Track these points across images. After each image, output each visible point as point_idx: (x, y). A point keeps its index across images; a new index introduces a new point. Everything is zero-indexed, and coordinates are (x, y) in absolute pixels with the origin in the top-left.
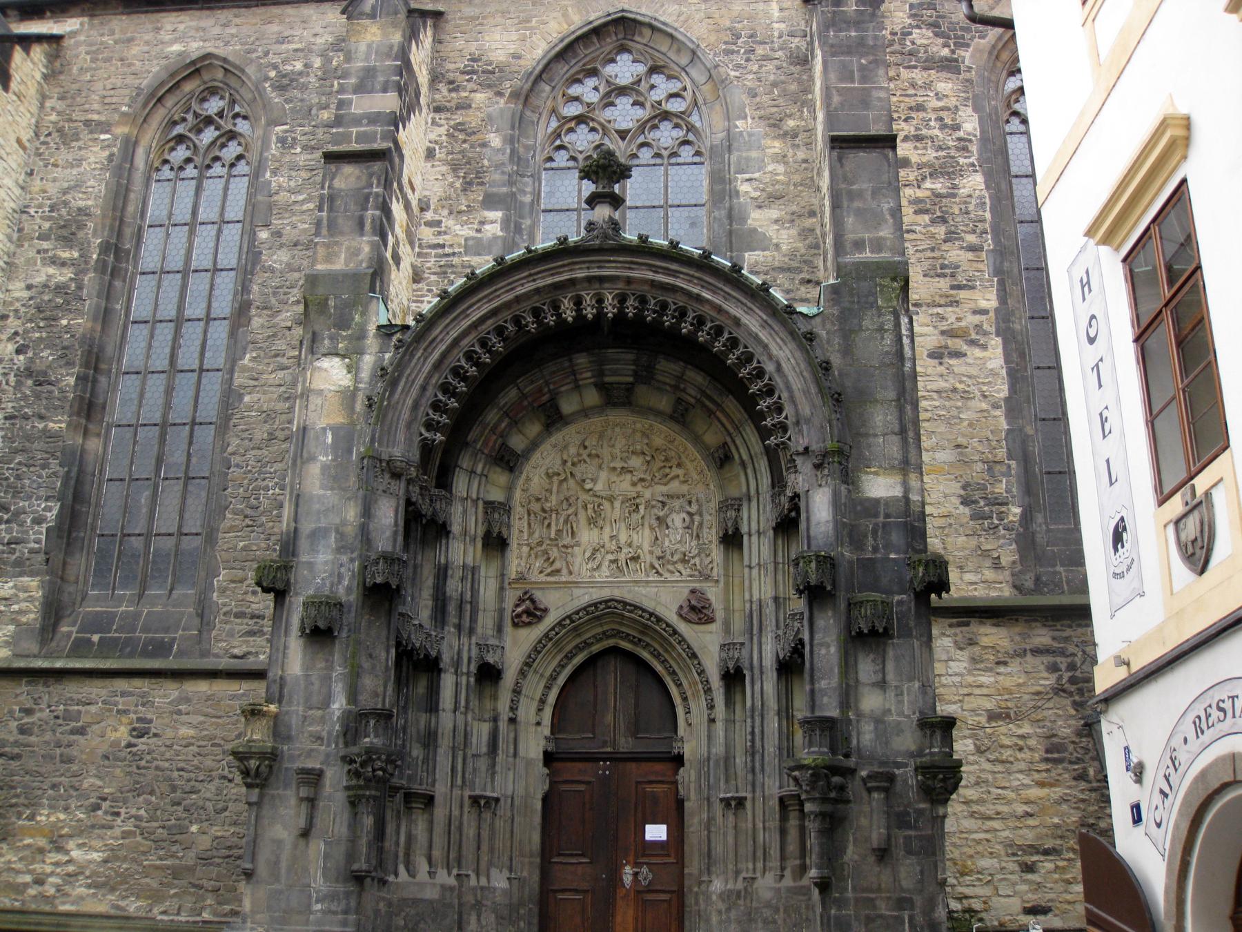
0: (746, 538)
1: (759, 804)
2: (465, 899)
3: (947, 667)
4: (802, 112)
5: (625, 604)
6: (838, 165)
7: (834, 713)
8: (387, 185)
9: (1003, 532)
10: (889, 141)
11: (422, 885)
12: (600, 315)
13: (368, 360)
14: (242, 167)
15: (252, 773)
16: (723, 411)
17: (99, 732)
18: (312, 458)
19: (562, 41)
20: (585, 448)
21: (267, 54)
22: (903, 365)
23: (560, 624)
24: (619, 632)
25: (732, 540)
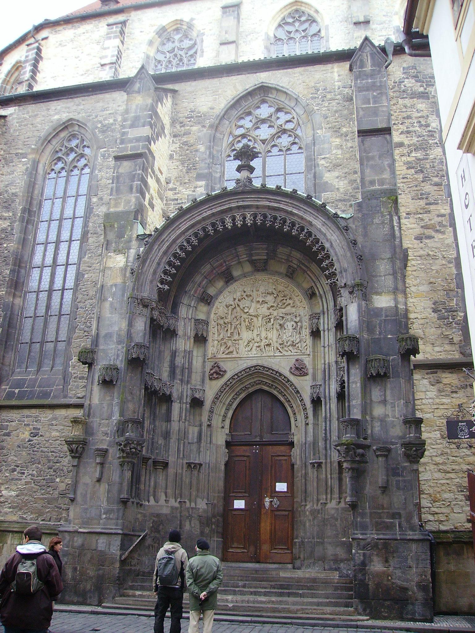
0: (322, 332)
1: (329, 465)
2: (183, 514)
3: (426, 395)
4: (350, 124)
5: (264, 367)
6: (362, 144)
7: (359, 417)
8: (145, 169)
9: (454, 325)
10: (387, 131)
11: (162, 506)
12: (244, 225)
13: (133, 252)
14: (87, 170)
15: (74, 451)
16: (310, 270)
17: (16, 435)
18: (105, 300)
19: (233, 99)
20: (245, 292)
21: (96, 117)
22: (395, 240)
23: (232, 378)
24: (262, 381)
25: (316, 334)
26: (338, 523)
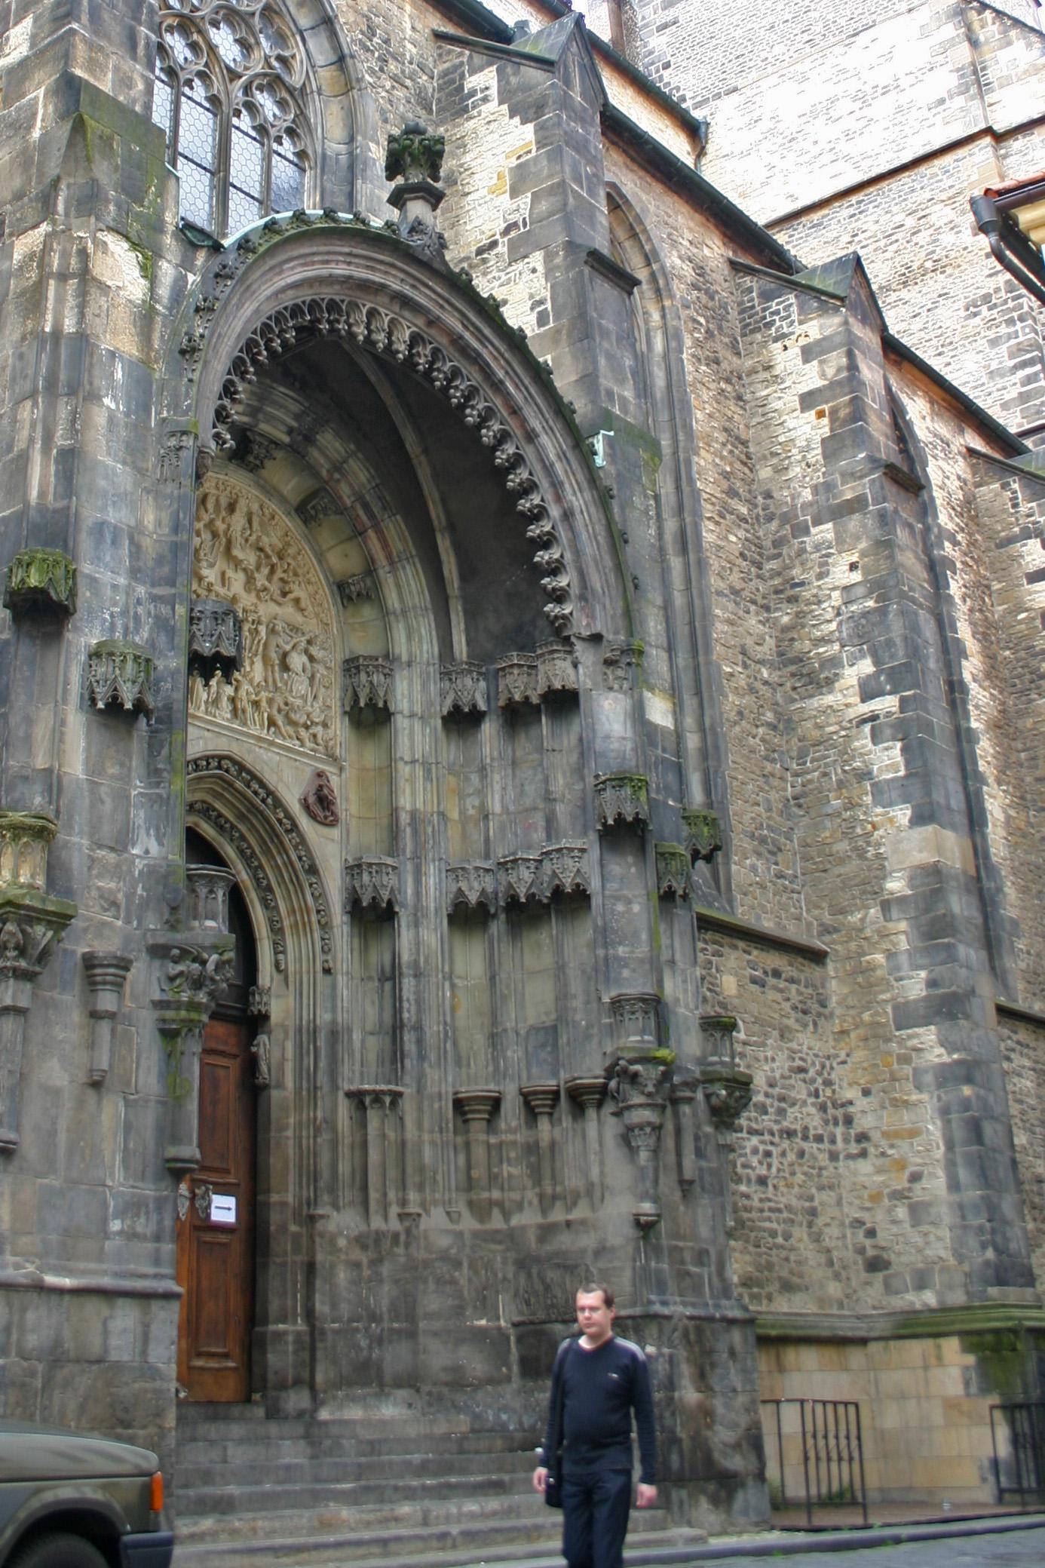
26: (463, 1276)
